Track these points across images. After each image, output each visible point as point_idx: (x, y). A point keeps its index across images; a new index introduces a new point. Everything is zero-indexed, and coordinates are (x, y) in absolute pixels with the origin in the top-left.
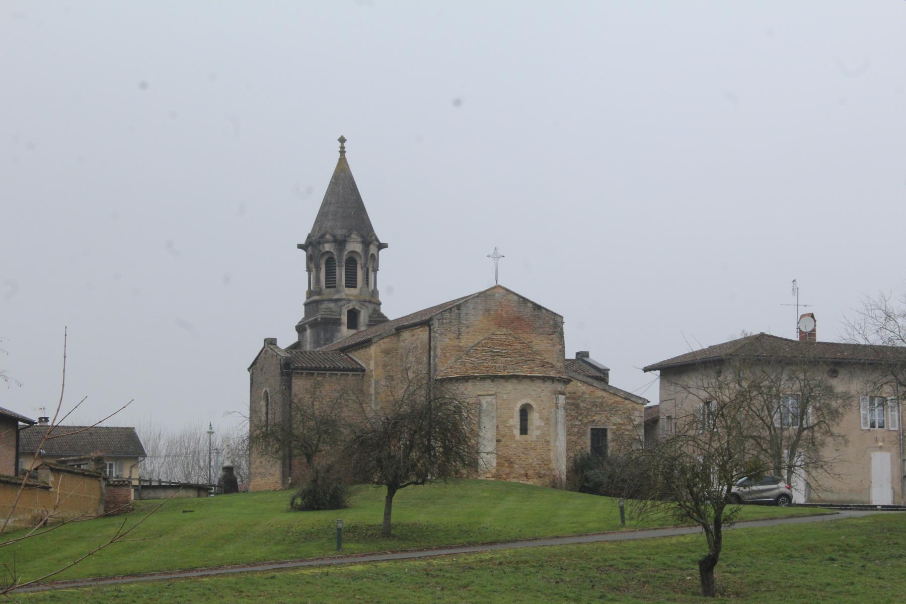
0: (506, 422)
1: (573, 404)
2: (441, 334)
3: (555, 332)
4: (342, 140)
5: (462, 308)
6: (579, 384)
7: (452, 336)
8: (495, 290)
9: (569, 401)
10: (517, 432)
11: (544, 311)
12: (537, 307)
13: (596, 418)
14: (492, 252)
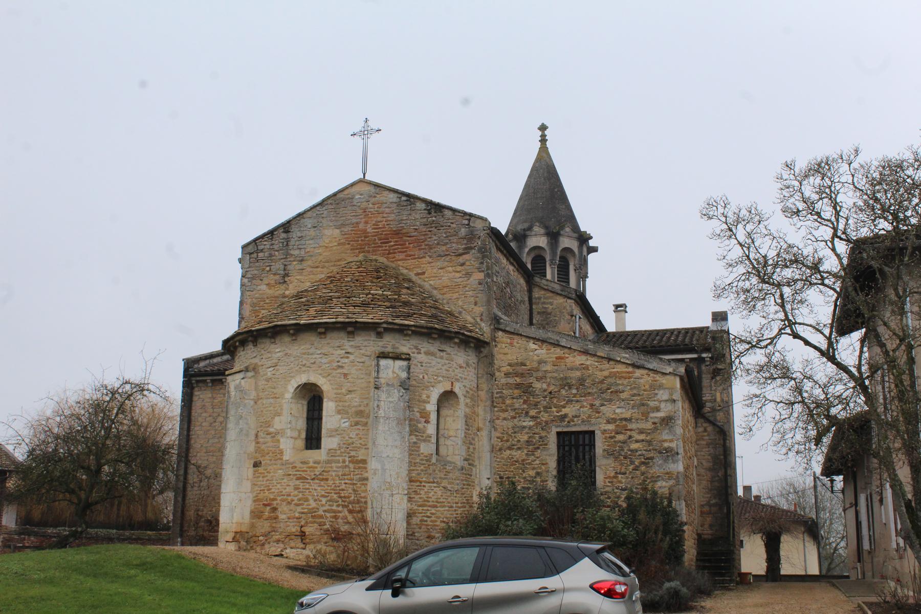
0: (268, 424)
1: (518, 386)
2: (253, 278)
3: (467, 250)
4: (543, 128)
5: (294, 228)
6: (532, 346)
10: (290, 445)
11: (448, 213)
12: (435, 208)
13: (569, 410)
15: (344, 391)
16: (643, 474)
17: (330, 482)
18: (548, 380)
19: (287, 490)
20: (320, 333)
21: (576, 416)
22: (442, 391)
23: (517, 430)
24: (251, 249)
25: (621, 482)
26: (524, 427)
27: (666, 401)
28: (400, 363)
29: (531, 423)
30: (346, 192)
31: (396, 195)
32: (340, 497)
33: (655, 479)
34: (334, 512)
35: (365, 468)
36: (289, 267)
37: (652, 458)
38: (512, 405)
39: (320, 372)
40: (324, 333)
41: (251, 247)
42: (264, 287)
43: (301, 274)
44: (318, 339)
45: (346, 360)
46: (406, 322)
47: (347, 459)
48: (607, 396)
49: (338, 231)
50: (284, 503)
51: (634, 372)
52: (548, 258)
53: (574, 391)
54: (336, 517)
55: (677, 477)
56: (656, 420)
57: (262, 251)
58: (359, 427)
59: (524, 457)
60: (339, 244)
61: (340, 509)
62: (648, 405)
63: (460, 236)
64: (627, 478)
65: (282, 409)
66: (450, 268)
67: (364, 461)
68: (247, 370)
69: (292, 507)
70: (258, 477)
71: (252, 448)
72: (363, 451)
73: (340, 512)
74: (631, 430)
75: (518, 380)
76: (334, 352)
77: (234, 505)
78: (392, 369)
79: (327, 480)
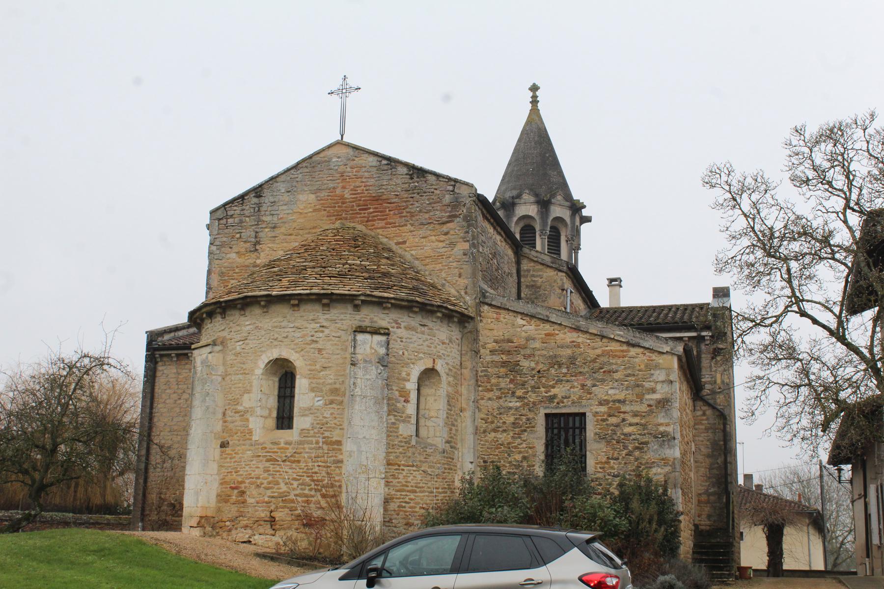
0: (237, 402)
1: (504, 364)
2: (222, 245)
3: (452, 218)
4: (534, 88)
5: (266, 192)
6: (520, 321)
7: (242, 246)
8: (330, 152)
9: (496, 358)
14: (336, 85)
15: (318, 367)
16: (637, 459)
17: (303, 465)
18: (537, 358)
19: (257, 472)
20: (294, 305)
21: (566, 397)
22: (423, 368)
23: (502, 410)
24: (220, 214)
25: (613, 468)
26: (510, 408)
27: (663, 382)
28: (378, 338)
29: (518, 404)
30: (322, 155)
31: (376, 159)
32: (313, 481)
33: (650, 465)
34: (306, 496)
35: (340, 450)
36: (261, 235)
37: (646, 443)
38: (497, 384)
39: (292, 346)
40: (298, 305)
41: (220, 212)
42: (233, 256)
43: (274, 242)
44: (291, 312)
45: (321, 335)
46: (386, 295)
47: (321, 440)
48: (599, 376)
49: (313, 196)
50: (253, 487)
51: (628, 351)
52: (538, 227)
53: (564, 370)
54: (308, 502)
55: (674, 463)
56: (652, 403)
57: (232, 216)
58: (334, 406)
59: (510, 440)
60: (314, 211)
61: (313, 493)
62: (643, 386)
63: (444, 203)
64: (620, 463)
65: (251, 386)
66: (433, 238)
67: (339, 443)
68: (214, 343)
69: (261, 490)
70: (226, 458)
71: (219, 427)
72: (338, 431)
73: (313, 496)
74: (624, 413)
75: (505, 358)
76: (308, 325)
77: (199, 487)
78: (369, 345)
79: (299, 462)
